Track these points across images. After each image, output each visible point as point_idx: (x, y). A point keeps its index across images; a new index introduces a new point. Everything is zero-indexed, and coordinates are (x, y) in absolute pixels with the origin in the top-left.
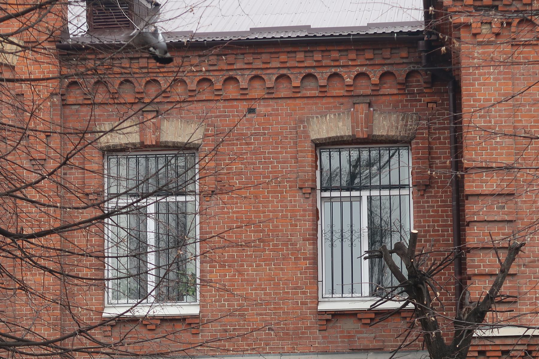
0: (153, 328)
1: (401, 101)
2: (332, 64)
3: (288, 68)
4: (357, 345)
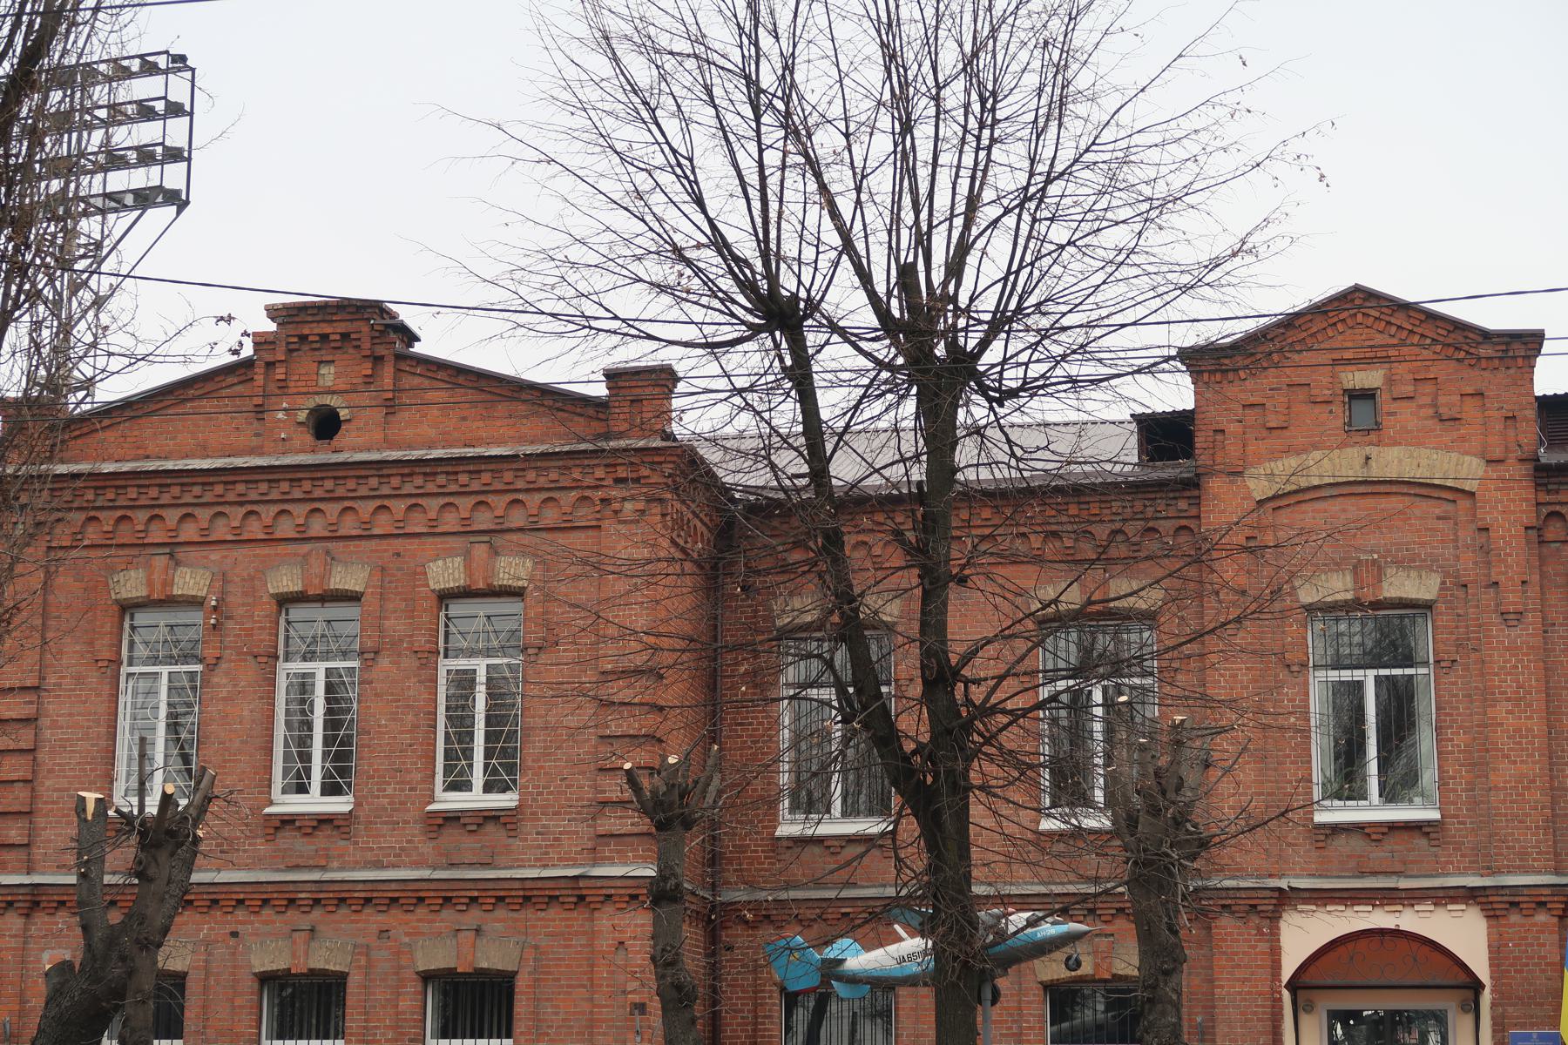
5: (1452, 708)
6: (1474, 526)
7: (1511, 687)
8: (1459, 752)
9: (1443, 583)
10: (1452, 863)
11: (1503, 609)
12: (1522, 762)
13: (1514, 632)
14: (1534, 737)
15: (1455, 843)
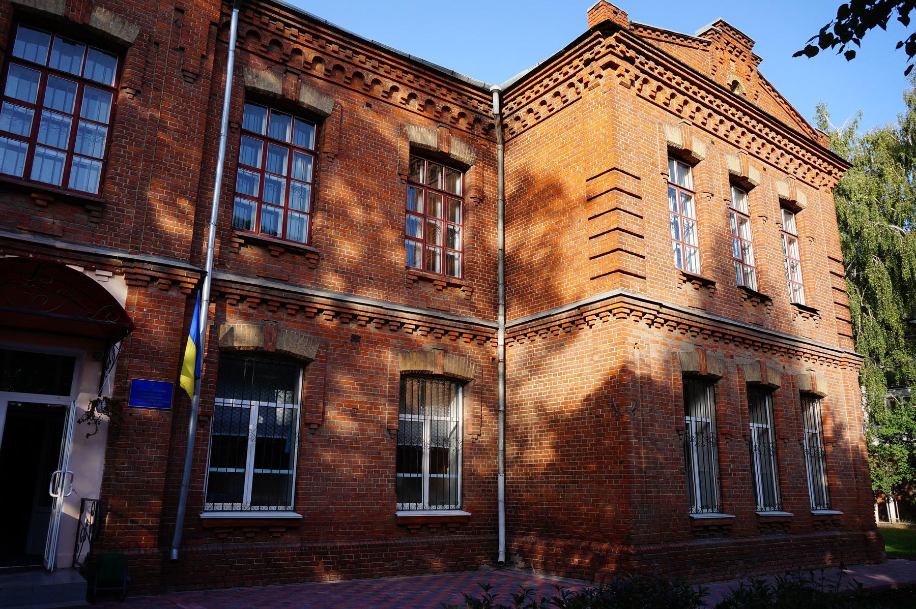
0: (277, 254)
1: (466, 137)
2: (430, 92)
3: (400, 83)
4: (432, 305)
5: (129, 124)
6: (173, 7)
7: (179, 122)
8: (129, 158)
9: (140, 34)
10: (106, 239)
11: (185, 67)
12: (178, 177)
13: (189, 87)
14: (191, 162)
15: (112, 224)
